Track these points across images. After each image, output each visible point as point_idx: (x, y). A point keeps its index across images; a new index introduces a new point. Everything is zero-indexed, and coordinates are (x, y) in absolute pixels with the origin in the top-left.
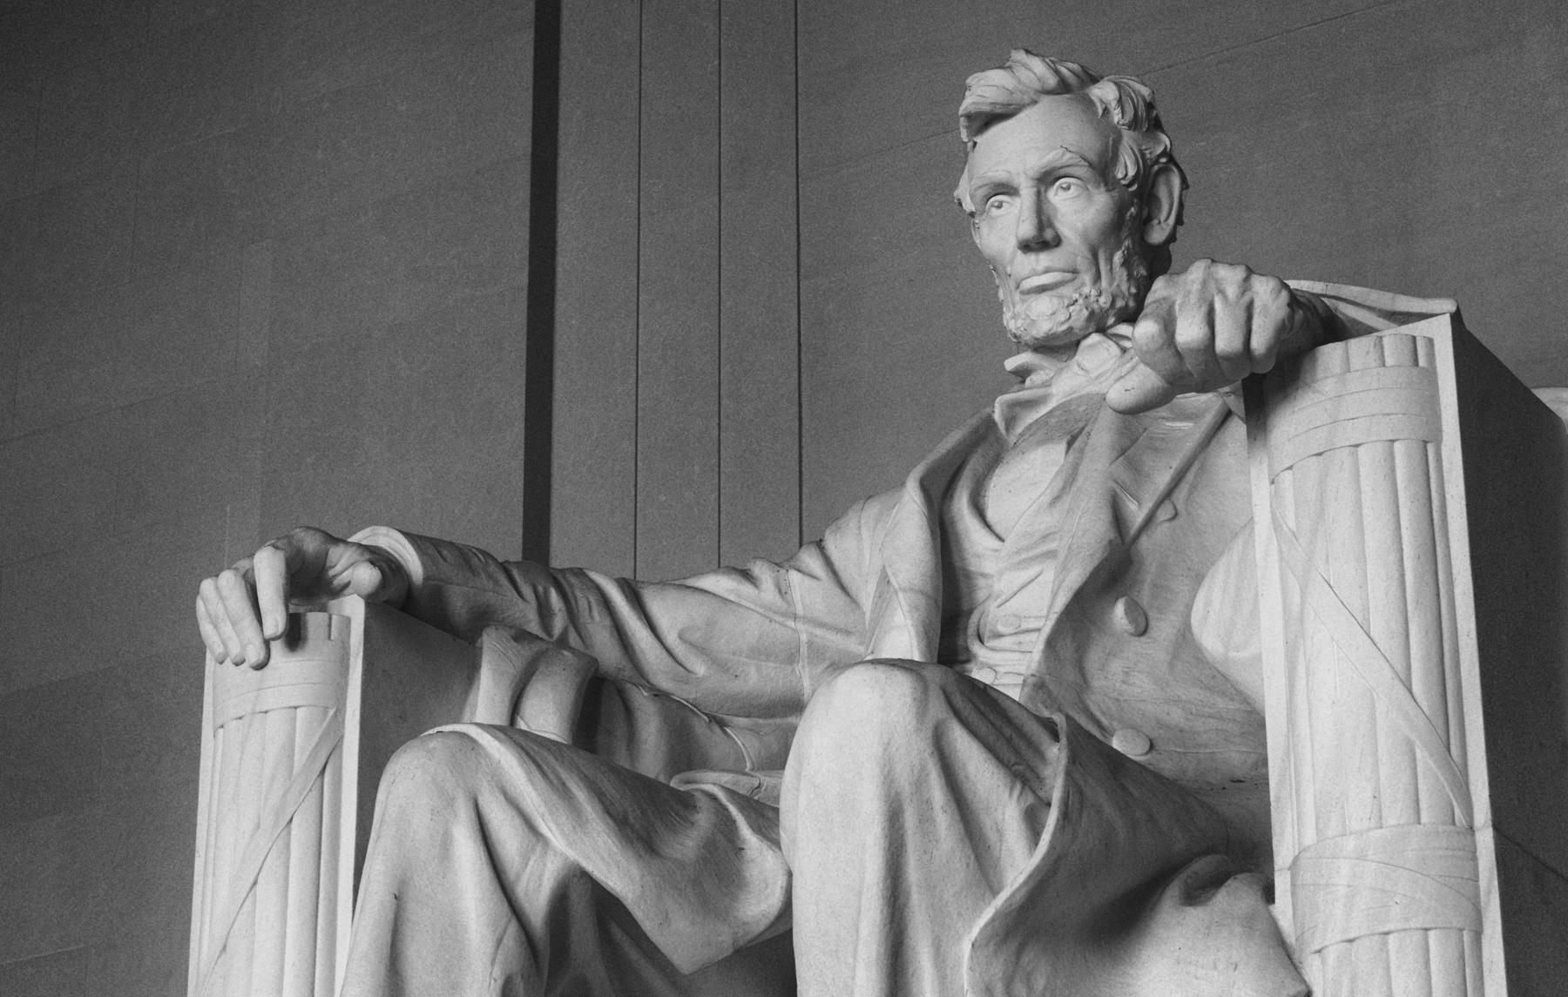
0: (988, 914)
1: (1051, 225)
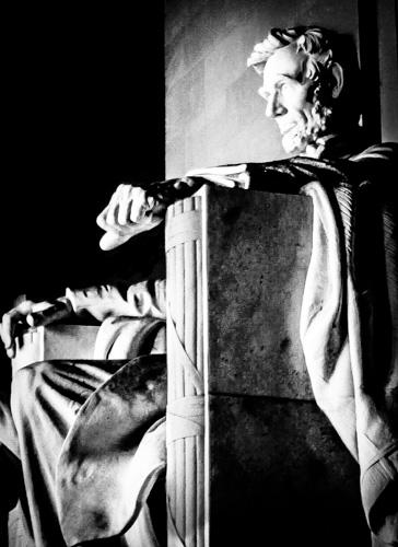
1: (281, 106)
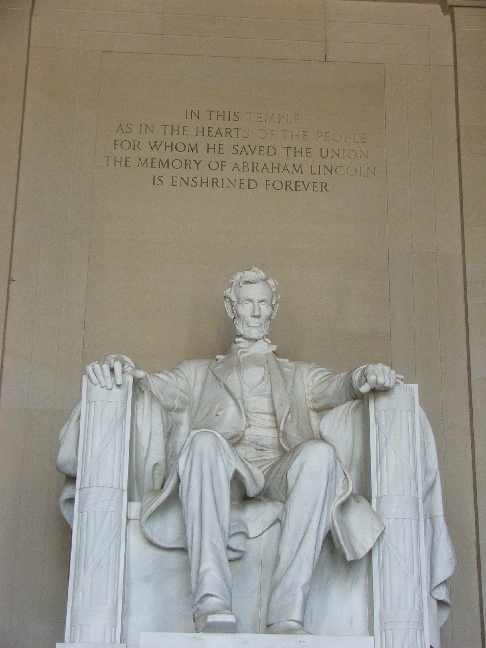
0: (339, 502)
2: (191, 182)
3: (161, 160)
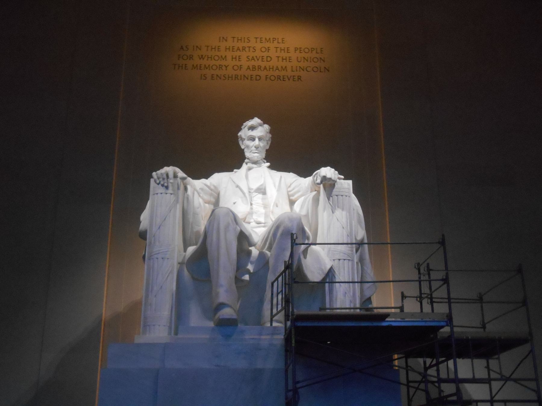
2: (223, 78)
3: (205, 65)
